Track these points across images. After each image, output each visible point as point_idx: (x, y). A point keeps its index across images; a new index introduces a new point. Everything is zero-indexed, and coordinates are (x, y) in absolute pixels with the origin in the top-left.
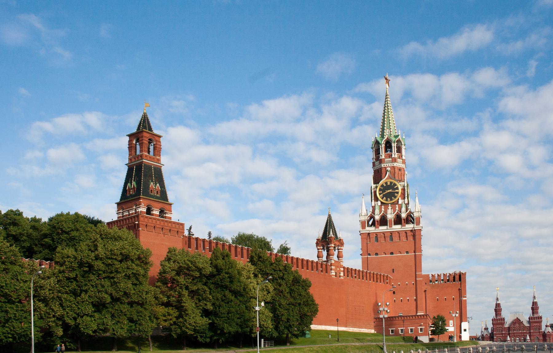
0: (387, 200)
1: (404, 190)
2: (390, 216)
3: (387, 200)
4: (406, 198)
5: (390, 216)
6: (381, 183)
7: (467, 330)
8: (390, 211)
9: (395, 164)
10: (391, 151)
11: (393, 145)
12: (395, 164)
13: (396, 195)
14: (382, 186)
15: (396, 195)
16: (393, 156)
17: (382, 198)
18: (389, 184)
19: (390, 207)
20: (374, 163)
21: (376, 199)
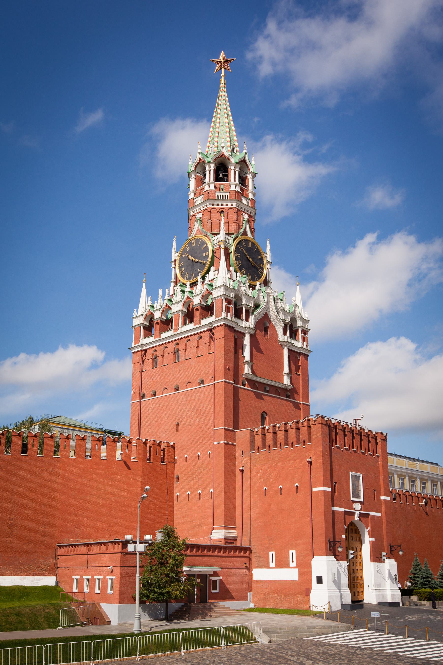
3: (189, 279)
12: (209, 204)
17: (183, 277)
18: (194, 245)
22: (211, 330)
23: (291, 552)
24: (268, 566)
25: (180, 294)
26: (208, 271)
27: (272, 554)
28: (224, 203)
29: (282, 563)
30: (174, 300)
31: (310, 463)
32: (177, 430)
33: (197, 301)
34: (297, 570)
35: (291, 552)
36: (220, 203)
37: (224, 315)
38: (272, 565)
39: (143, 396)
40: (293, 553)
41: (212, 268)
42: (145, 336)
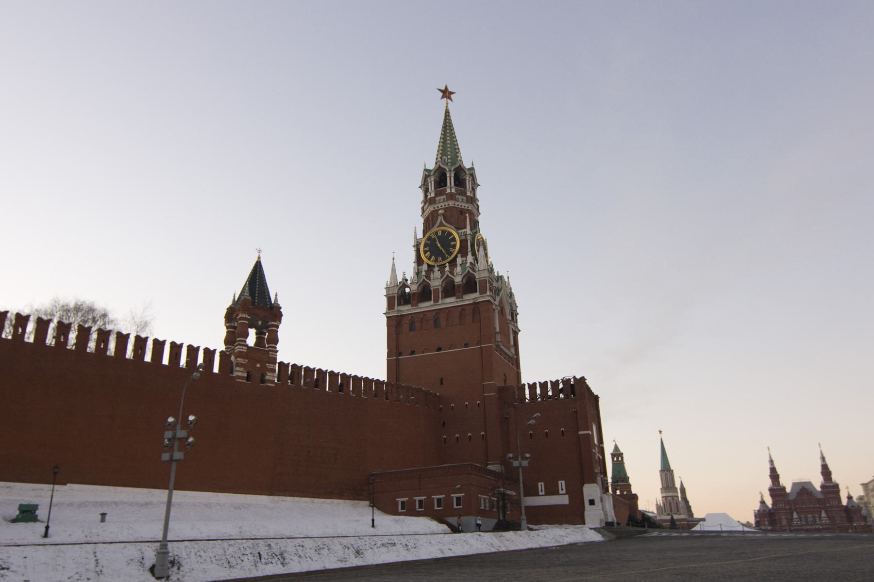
0: (436, 261)
1: (464, 243)
2: (436, 282)
4: (470, 254)
5: (436, 282)
6: (427, 235)
7: (597, 501)
8: (437, 273)
9: (451, 203)
10: (446, 185)
11: (448, 175)
12: (451, 203)
13: (452, 250)
14: (429, 238)
15: (452, 250)
16: (448, 191)
17: (429, 259)
18: (440, 234)
19: (436, 269)
20: (423, 208)
21: (419, 261)
22: (475, 303)
23: (560, 482)
24: (537, 494)
25: (437, 273)
26: (456, 257)
27: (541, 485)
28: (464, 205)
29: (552, 491)
30: (432, 276)
31: (576, 412)
32: (442, 384)
33: (458, 280)
34: (567, 497)
35: (560, 482)
36: (460, 204)
37: (488, 293)
38: (543, 493)
39: (400, 354)
40: (562, 484)
41: (459, 255)
42: (399, 304)
